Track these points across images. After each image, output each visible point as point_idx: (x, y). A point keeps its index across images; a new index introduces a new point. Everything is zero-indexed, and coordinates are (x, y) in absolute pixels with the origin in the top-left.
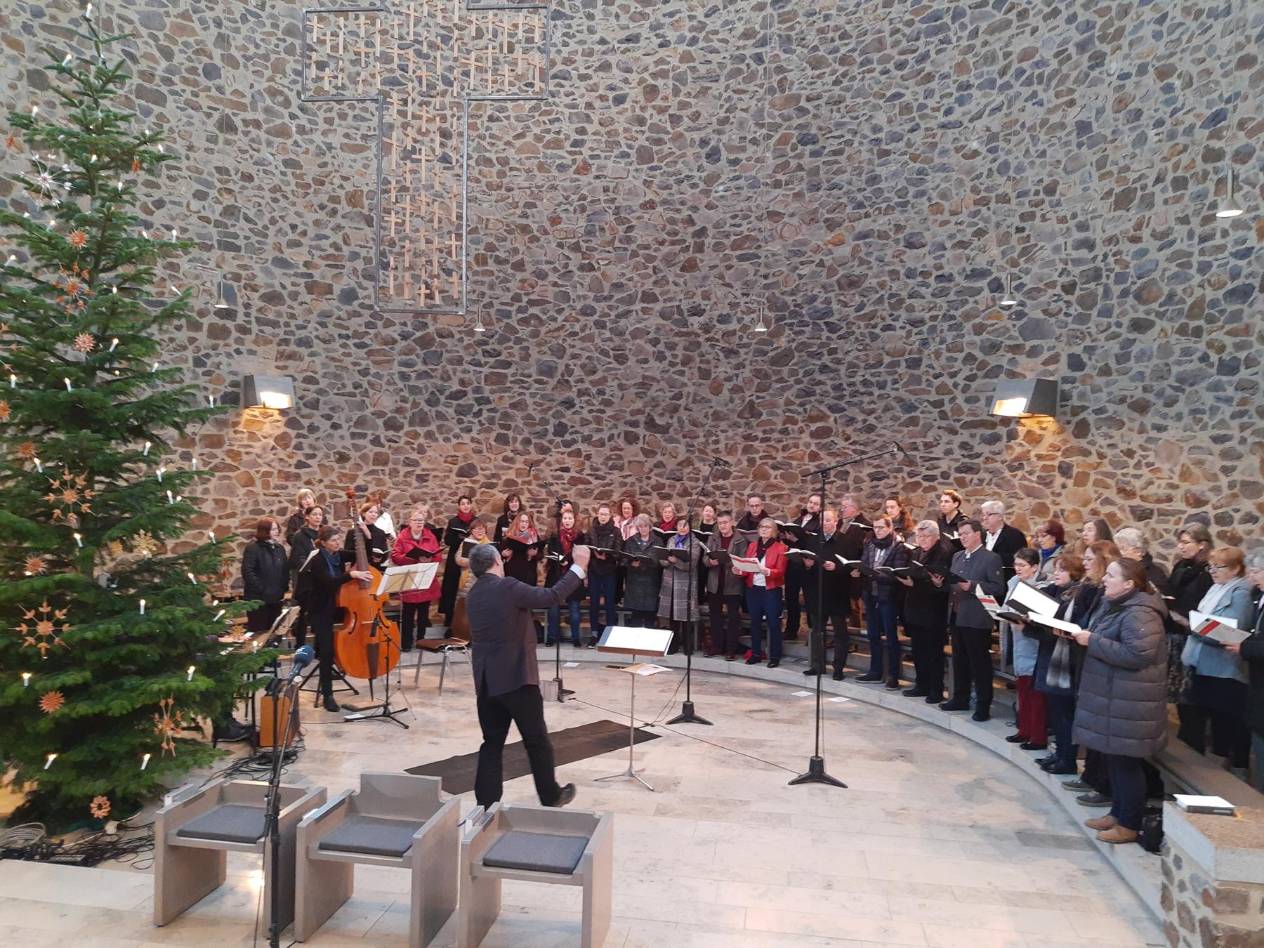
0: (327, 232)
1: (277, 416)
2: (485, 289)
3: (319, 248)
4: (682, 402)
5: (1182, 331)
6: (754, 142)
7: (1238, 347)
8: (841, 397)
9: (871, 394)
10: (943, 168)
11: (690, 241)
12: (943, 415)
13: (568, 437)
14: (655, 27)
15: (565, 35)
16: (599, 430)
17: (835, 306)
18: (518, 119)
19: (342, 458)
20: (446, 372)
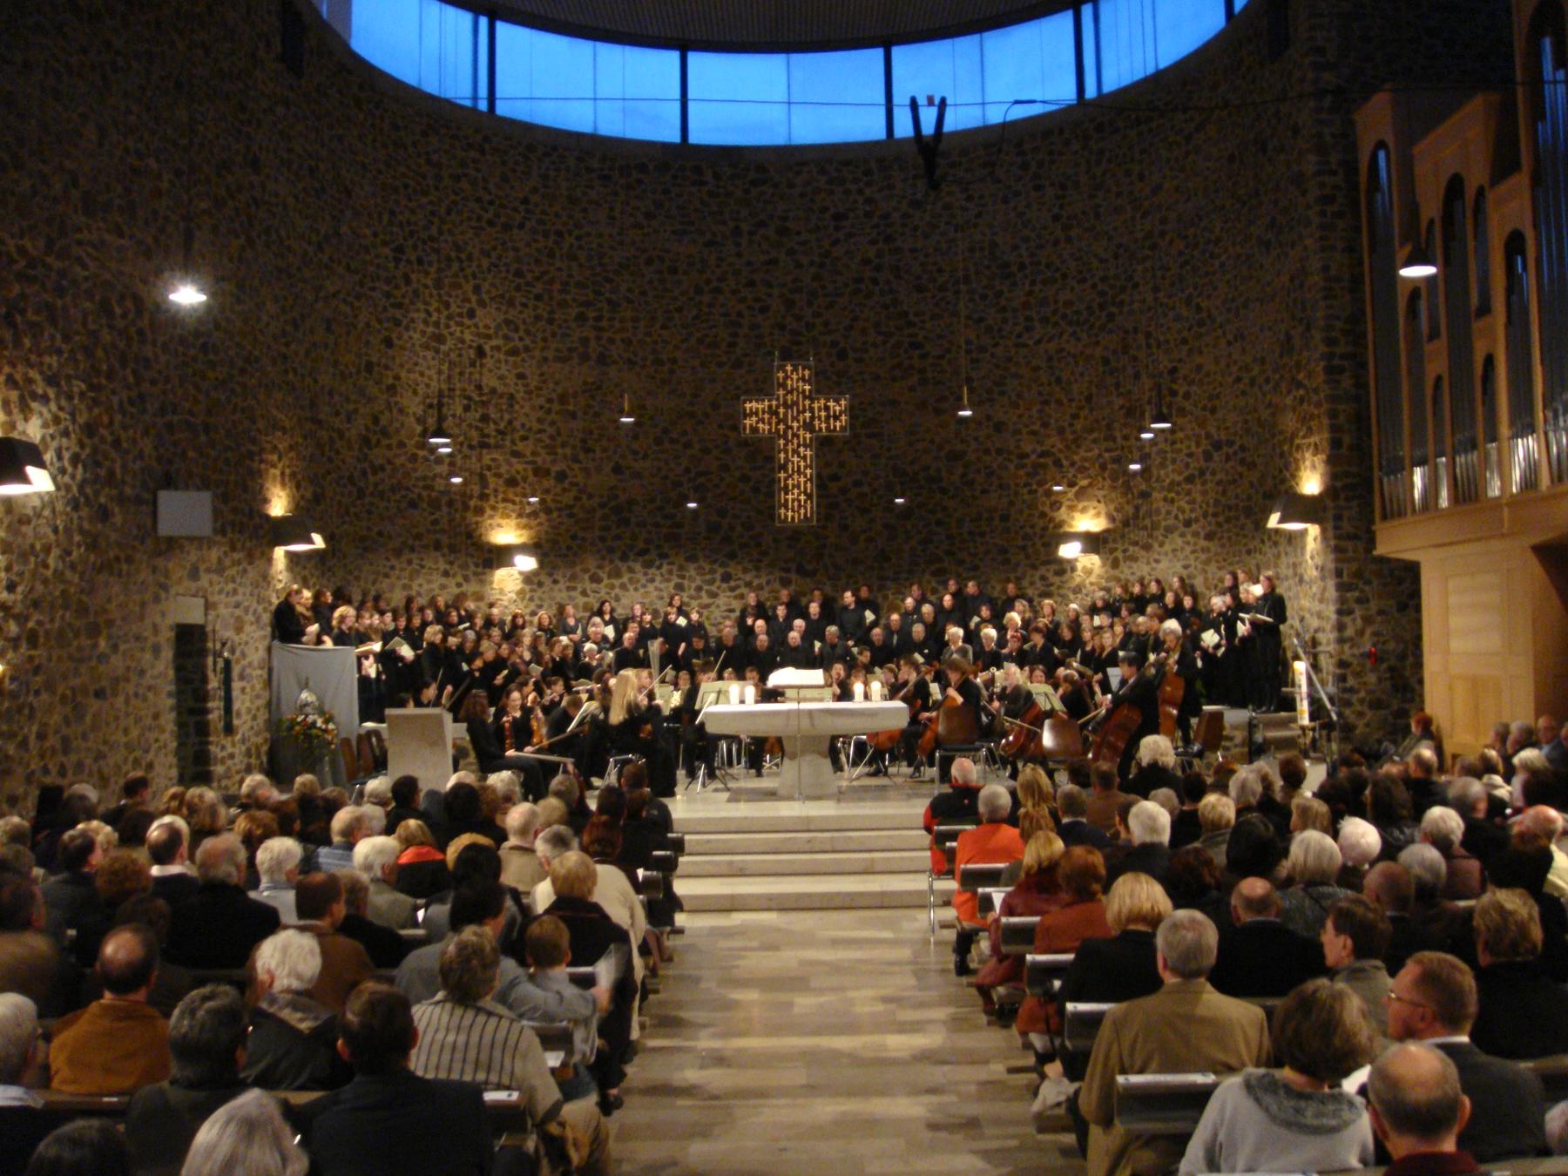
0: (545, 426)
3: (540, 440)
5: (1165, 499)
6: (875, 345)
7: (1192, 511)
14: (791, 252)
18: (684, 327)
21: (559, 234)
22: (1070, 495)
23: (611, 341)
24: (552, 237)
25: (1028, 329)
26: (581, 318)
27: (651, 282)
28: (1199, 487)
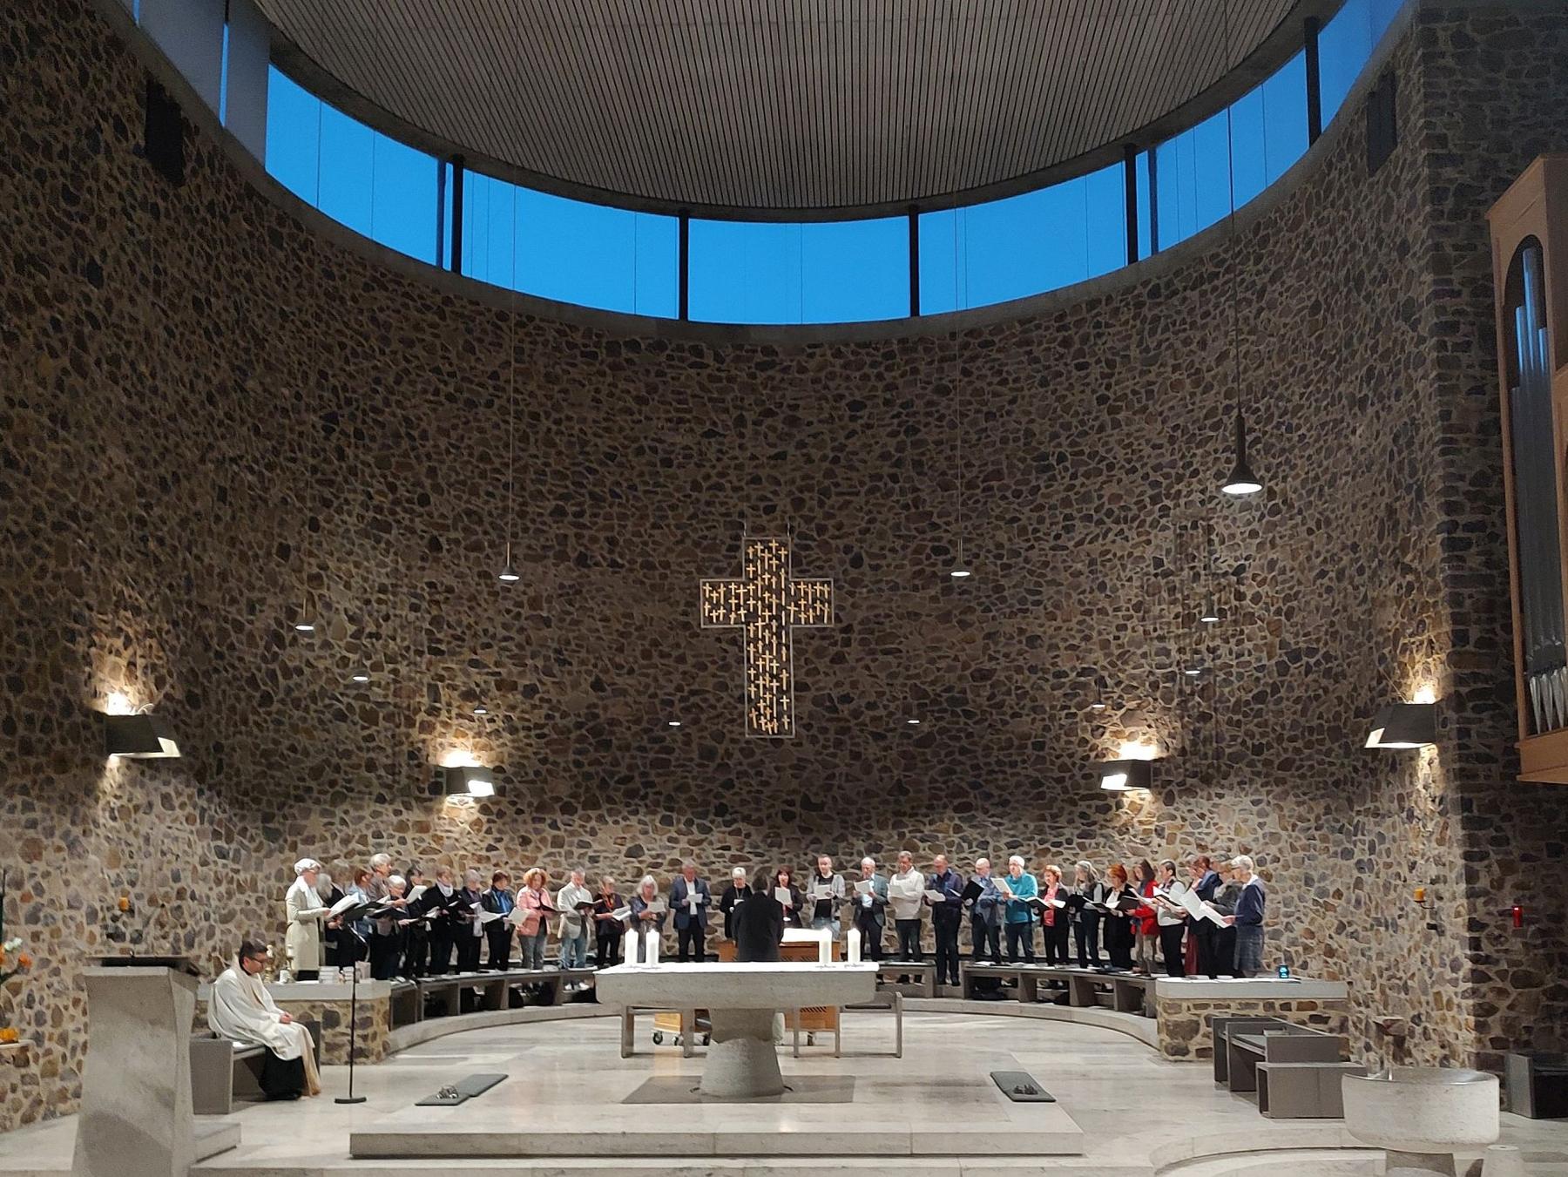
0: (513, 634)
1: (472, 804)
2: (649, 681)
3: (506, 649)
4: (836, 782)
5: (1229, 723)
6: (893, 550)
7: (1263, 735)
8: (979, 776)
9: (1004, 772)
10: (1053, 582)
11: (839, 637)
12: (1065, 791)
13: (728, 817)
14: (802, 445)
15: (720, 451)
16: (758, 810)
17: (970, 696)
18: (678, 527)
19: (525, 841)
20: (616, 759)
21: (535, 416)
22: (1115, 719)
23: (594, 540)
24: (527, 419)
25: (1068, 529)
26: (559, 512)
27: (641, 474)
28: (1271, 707)
